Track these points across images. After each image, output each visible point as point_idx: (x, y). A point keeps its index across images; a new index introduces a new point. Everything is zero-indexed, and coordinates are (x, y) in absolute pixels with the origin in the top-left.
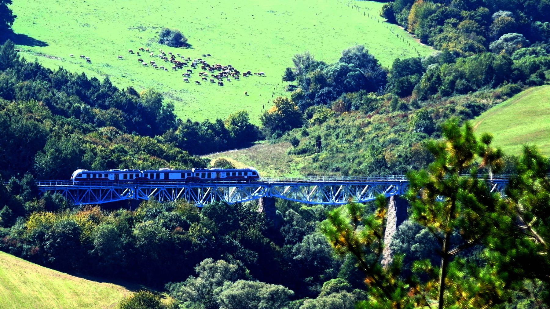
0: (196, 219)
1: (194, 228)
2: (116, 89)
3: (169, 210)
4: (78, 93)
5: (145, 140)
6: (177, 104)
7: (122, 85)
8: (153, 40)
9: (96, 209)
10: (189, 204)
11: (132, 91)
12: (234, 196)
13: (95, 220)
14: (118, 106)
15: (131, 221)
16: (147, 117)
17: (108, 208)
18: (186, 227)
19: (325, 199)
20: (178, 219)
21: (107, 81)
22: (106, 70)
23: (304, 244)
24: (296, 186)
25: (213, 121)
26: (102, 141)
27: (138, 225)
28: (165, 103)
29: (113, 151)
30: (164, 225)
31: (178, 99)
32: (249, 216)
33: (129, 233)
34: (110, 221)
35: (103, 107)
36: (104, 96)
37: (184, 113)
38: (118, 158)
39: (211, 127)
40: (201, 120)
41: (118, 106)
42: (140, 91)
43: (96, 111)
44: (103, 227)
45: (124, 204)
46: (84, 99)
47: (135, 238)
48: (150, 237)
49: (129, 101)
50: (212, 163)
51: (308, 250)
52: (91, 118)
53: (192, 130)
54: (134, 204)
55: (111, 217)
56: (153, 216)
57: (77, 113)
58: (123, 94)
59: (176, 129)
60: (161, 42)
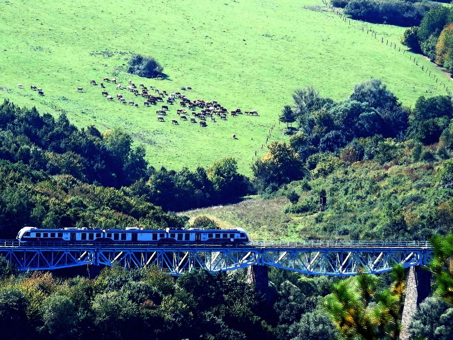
0: (169, 291)
1: (167, 302)
2: (74, 128)
3: (137, 278)
4: (27, 132)
5: (109, 191)
6: (149, 149)
7: (81, 123)
8: (120, 68)
9: (47, 276)
10: (161, 272)
11: (94, 131)
12: (217, 263)
13: (46, 289)
14: (77, 149)
15: (90, 292)
16: (111, 163)
17: (61, 275)
18: (158, 300)
19: (329, 269)
20: (147, 290)
21: (63, 118)
22: (62, 105)
23: (302, 324)
24: (294, 252)
25: (193, 170)
26: (55, 192)
27: (98, 297)
28: (135, 145)
29: (69, 205)
30: (131, 297)
31: (151, 142)
32: (236, 287)
33: (87, 306)
34: (64, 292)
35: (58, 150)
36: (59, 136)
37: (156, 160)
38: (76, 214)
39: (191, 177)
40: (178, 168)
41: (77, 149)
42: (103, 131)
43: (49, 154)
44: (55, 298)
45: (81, 271)
46: (35, 139)
47: (94, 313)
48: (113, 312)
49: (90, 144)
50: (192, 222)
51: (307, 332)
52: (42, 164)
53: (167, 180)
54: (95, 271)
55: (65, 287)
56: (117, 286)
57: (26, 157)
58: (83, 135)
59: (147, 179)
60: (131, 71)
